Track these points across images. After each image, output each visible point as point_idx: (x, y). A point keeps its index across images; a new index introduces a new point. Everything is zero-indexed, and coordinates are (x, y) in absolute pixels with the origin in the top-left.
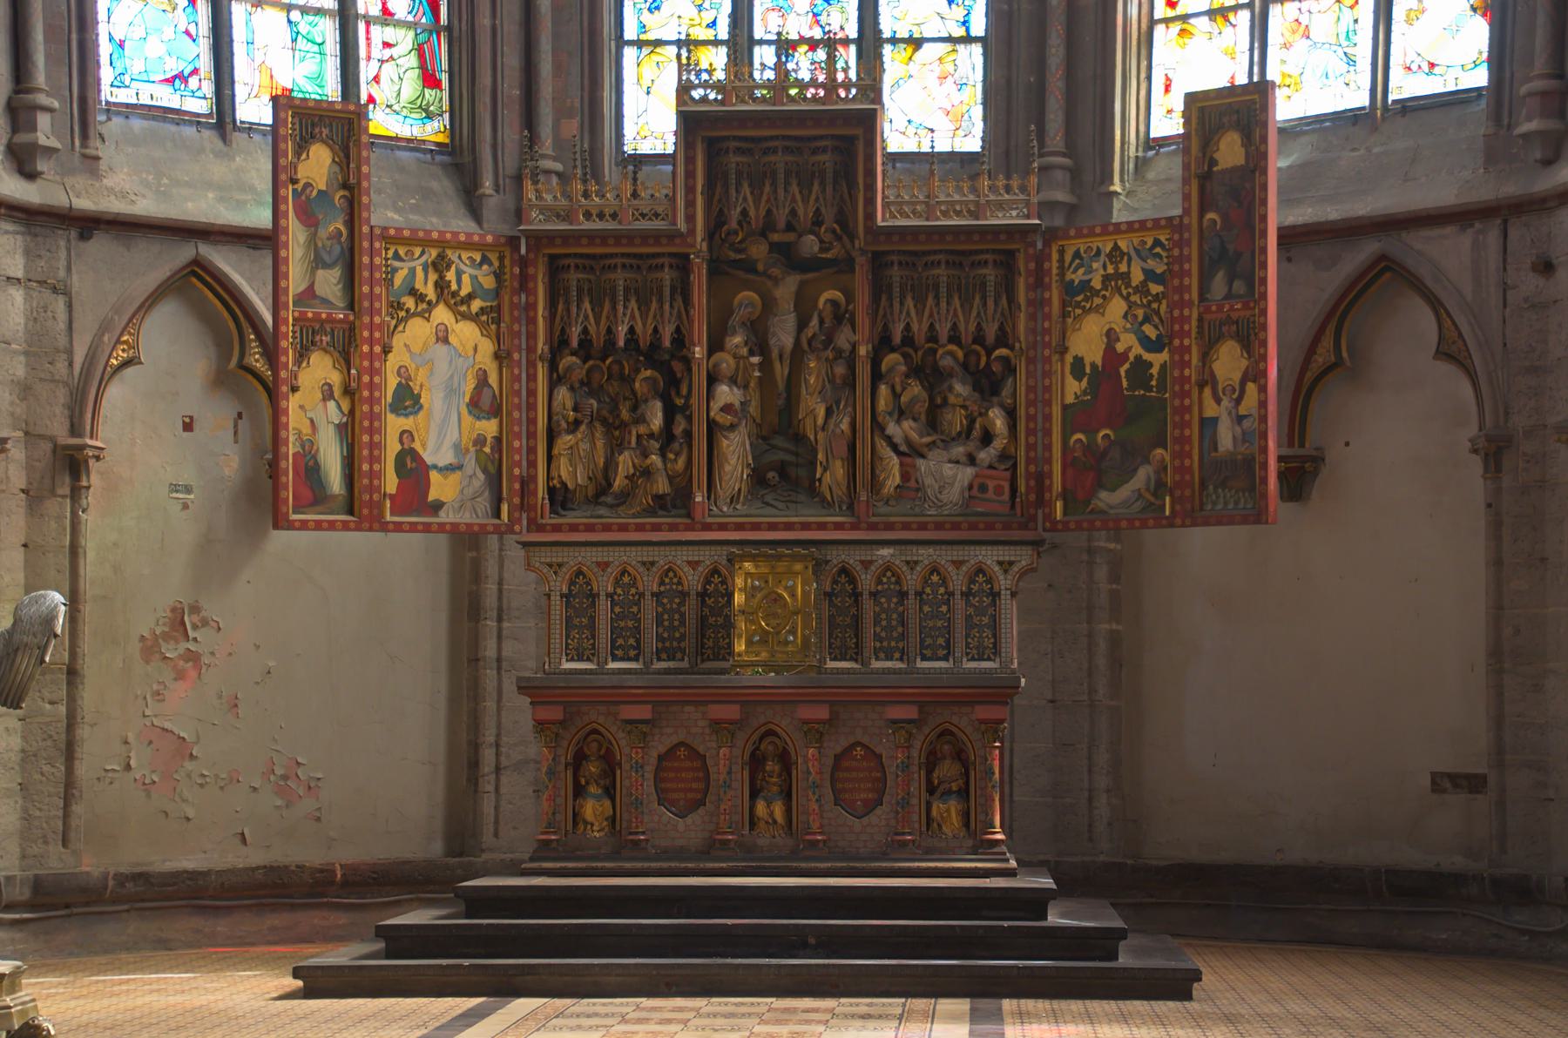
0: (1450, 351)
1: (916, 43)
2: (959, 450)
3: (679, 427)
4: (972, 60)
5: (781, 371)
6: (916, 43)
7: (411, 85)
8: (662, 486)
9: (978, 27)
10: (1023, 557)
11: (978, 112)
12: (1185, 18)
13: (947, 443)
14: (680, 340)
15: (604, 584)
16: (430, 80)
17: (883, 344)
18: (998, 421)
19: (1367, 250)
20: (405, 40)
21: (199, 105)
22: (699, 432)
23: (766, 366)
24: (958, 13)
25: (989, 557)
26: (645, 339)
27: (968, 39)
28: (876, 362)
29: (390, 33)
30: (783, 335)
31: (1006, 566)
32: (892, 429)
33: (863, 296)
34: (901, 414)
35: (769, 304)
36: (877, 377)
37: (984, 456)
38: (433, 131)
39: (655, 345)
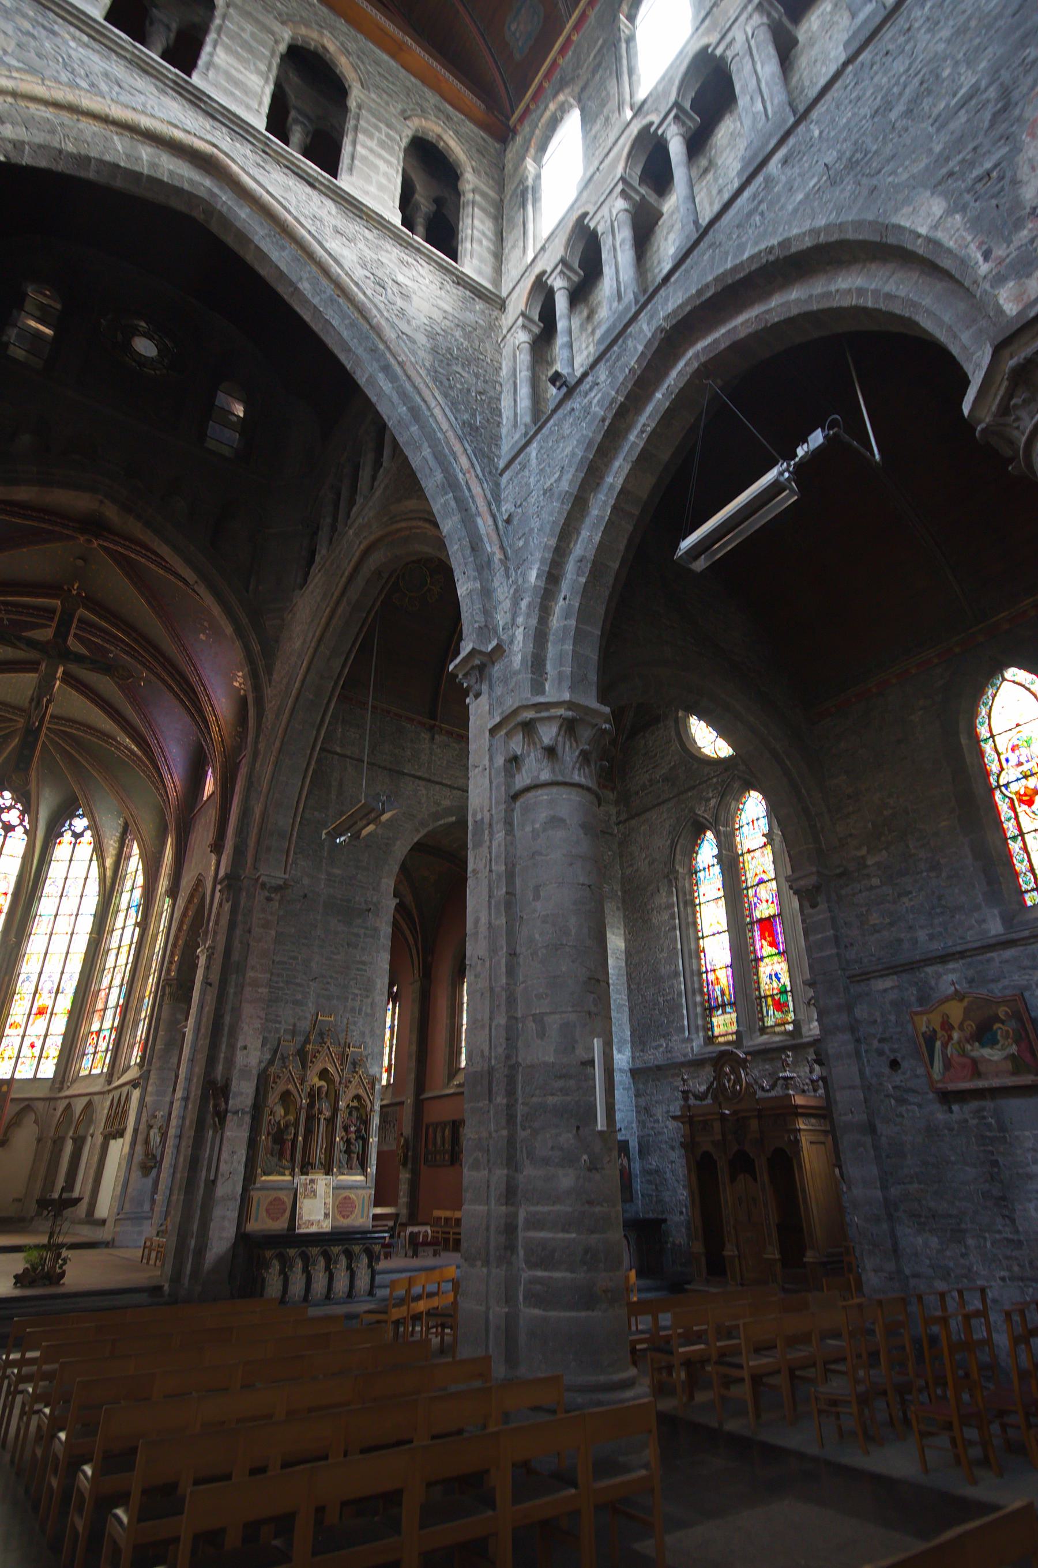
0: (36, 1122)
19: (26, 1103)
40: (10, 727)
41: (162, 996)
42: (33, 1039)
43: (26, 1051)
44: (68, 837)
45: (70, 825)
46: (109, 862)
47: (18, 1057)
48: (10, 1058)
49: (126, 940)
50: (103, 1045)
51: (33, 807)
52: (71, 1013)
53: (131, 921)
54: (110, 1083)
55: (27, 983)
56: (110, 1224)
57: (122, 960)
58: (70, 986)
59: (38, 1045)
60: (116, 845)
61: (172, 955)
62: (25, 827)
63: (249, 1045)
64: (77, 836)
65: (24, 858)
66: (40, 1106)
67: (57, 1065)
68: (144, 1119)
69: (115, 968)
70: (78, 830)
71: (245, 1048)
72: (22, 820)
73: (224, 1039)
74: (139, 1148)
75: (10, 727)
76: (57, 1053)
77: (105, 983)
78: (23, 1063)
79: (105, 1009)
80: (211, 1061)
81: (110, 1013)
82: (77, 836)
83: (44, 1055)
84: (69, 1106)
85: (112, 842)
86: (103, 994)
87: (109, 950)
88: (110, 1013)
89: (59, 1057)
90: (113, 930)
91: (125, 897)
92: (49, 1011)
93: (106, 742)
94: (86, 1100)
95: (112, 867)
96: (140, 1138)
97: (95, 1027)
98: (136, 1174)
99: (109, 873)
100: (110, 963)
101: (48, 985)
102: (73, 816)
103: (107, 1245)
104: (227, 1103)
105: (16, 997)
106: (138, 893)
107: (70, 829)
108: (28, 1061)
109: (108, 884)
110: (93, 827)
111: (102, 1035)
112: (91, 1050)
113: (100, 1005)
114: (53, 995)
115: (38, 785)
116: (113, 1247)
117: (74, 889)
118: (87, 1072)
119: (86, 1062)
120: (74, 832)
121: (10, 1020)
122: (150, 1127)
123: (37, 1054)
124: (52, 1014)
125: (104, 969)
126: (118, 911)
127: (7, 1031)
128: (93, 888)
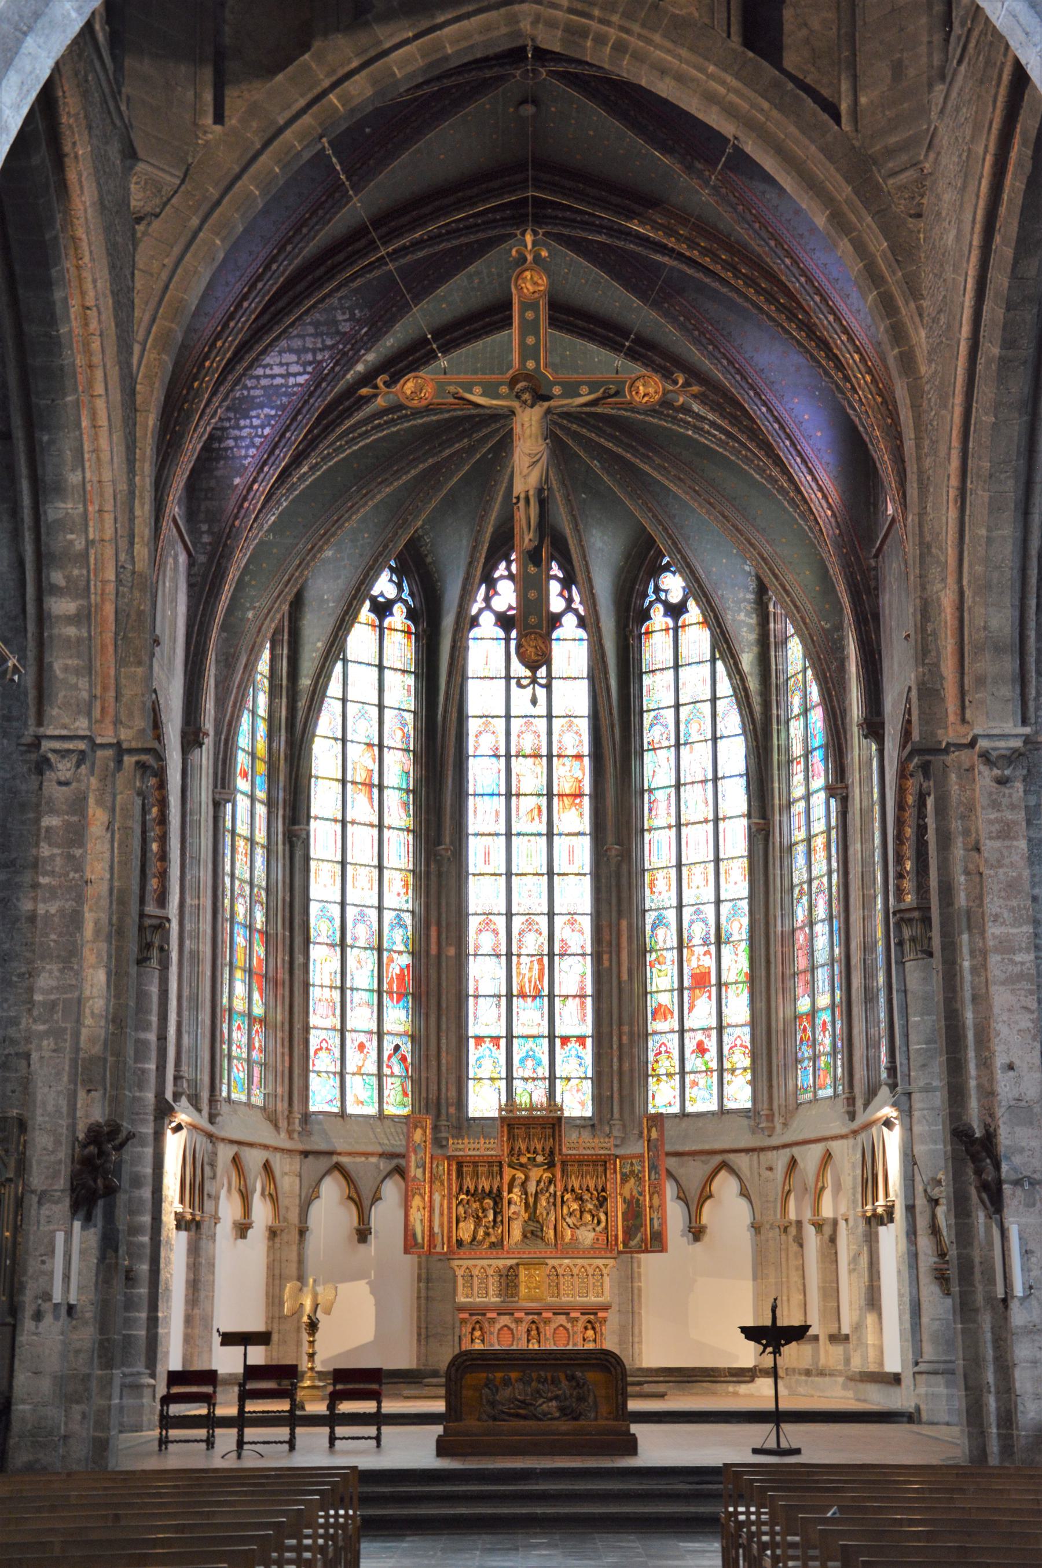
0: (744, 1193)
1: (569, 1079)
2: (590, 1227)
3: (499, 1219)
4: (588, 1084)
5: (531, 1200)
6: (569, 1079)
7: (399, 1097)
8: (493, 1239)
9: (590, 1074)
10: (611, 1262)
11: (590, 1103)
12: (658, 1075)
13: (585, 1225)
14: (500, 1190)
15: (475, 1272)
16: (405, 1094)
17: (566, 1190)
18: (603, 1217)
19: (717, 1159)
20: (397, 1081)
21: (336, 1110)
22: (506, 1220)
23: (526, 1199)
24: (583, 1069)
25: (600, 1262)
26: (487, 1190)
27: (586, 1078)
28: (562, 1197)
29: (393, 1080)
30: (532, 1188)
31: (606, 1266)
32: (568, 1220)
33: (559, 1175)
34: (571, 1214)
35: (527, 1178)
36: (563, 1202)
37: (598, 1229)
38: (405, 1111)
39: (491, 1192)
40: (497, 430)
41: (900, 944)
42: (700, 1036)
43: (693, 1062)
44: (659, 618)
45: (657, 590)
46: (747, 660)
47: (683, 1073)
48: (669, 1075)
49: (818, 826)
50: (825, 1042)
51: (580, 576)
52: (752, 979)
53: (818, 782)
54: (852, 1116)
55: (661, 932)
56: (907, 1380)
57: (820, 867)
58: (738, 927)
59: (712, 1045)
60: (753, 620)
61: (899, 859)
62: (576, 612)
63: (1017, 1063)
64: (675, 611)
65: (592, 678)
66: (742, 1162)
67: (753, 1083)
68: (919, 1188)
69: (810, 882)
70: (675, 597)
71: (1011, 1067)
72: (570, 601)
73: (971, 1054)
74: (925, 1243)
75: (497, 430)
76: (747, 1062)
77: (801, 914)
78: (695, 1084)
79: (813, 969)
80: (956, 1094)
81: (822, 975)
82: (675, 611)
83: (727, 1065)
84: (793, 1163)
85: (742, 616)
86: (801, 938)
87: (791, 846)
88: (822, 975)
89: (754, 1068)
90: (789, 804)
91: (796, 729)
92: (713, 981)
93: (675, 420)
94: (817, 1150)
95: (756, 670)
96: (922, 1223)
97: (804, 1005)
98: (930, 1290)
99: (753, 684)
100: (799, 875)
101: (697, 932)
102: (656, 571)
103: (910, 1417)
104: (997, 1166)
105: (650, 958)
106: (817, 717)
107: (658, 599)
108: (701, 1079)
109: (757, 708)
110: (697, 588)
111: (819, 1022)
112: (806, 1052)
113: (802, 963)
114: (713, 948)
115: (576, 528)
116: (920, 1422)
117: (697, 728)
118: (809, 1096)
119: (805, 1077)
120: (666, 604)
121: (652, 1003)
122: (935, 1202)
123: (714, 1065)
124: (719, 985)
125: (792, 887)
126: (789, 762)
127: (653, 1026)
128: (731, 721)
